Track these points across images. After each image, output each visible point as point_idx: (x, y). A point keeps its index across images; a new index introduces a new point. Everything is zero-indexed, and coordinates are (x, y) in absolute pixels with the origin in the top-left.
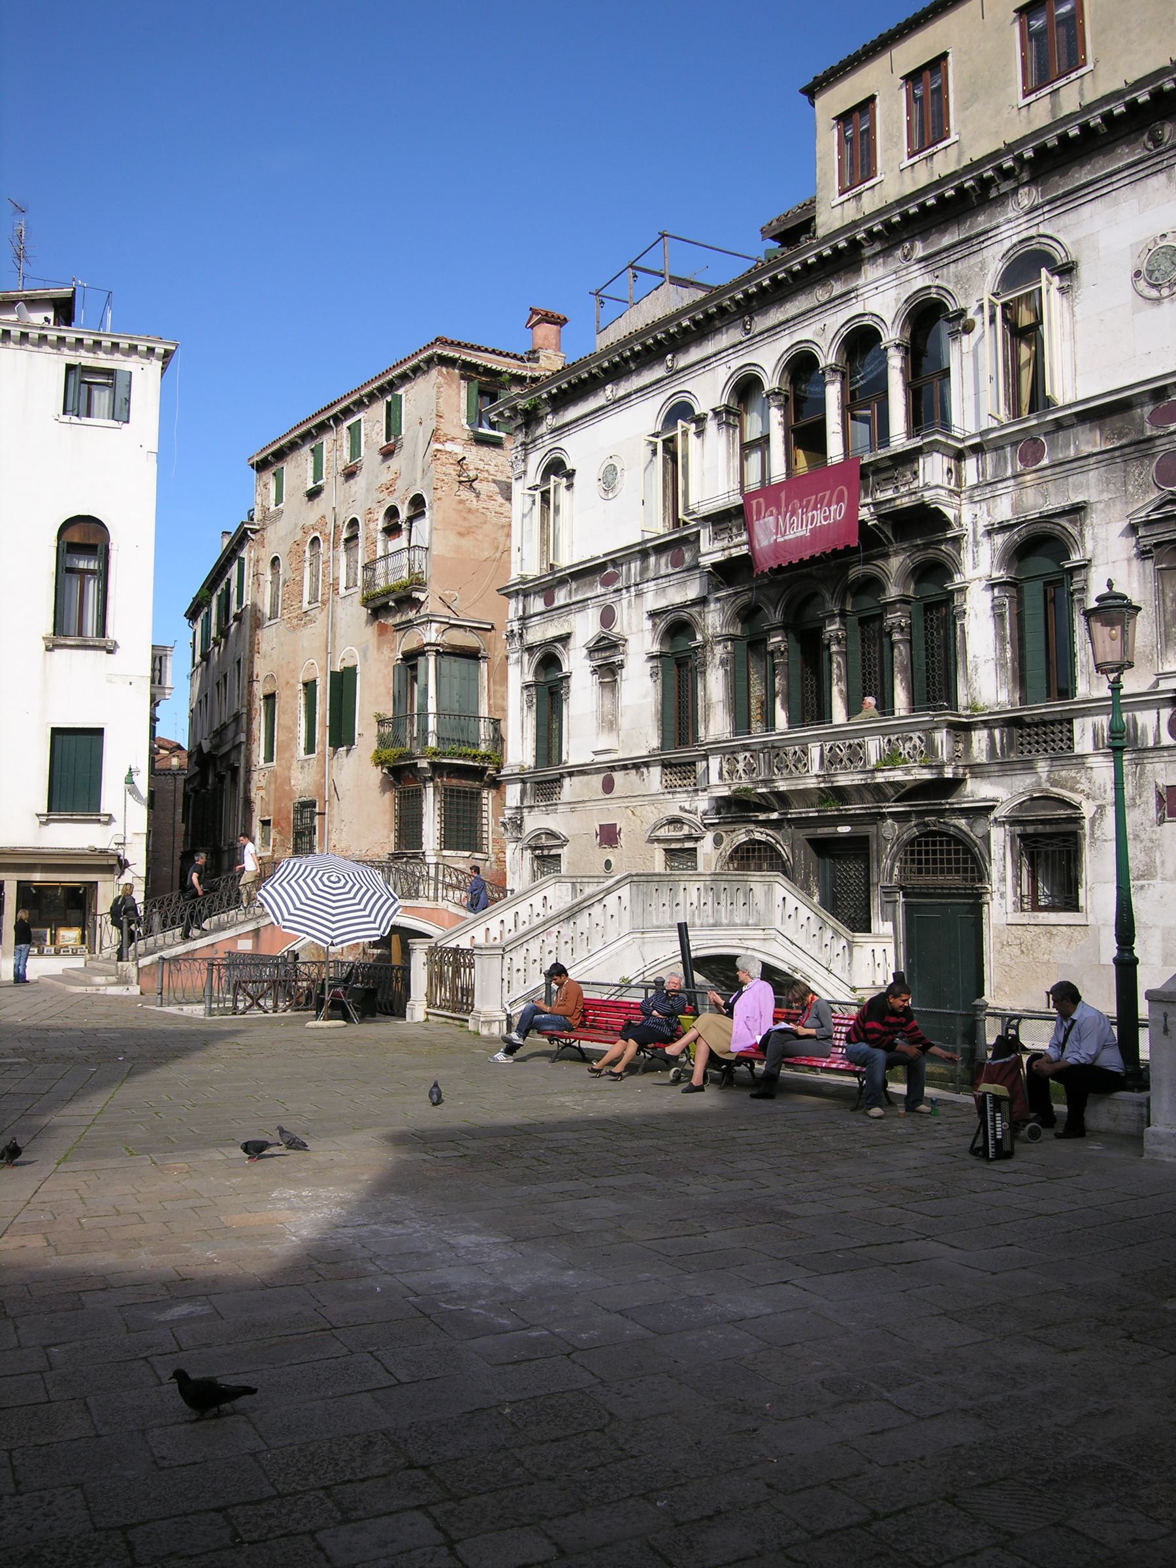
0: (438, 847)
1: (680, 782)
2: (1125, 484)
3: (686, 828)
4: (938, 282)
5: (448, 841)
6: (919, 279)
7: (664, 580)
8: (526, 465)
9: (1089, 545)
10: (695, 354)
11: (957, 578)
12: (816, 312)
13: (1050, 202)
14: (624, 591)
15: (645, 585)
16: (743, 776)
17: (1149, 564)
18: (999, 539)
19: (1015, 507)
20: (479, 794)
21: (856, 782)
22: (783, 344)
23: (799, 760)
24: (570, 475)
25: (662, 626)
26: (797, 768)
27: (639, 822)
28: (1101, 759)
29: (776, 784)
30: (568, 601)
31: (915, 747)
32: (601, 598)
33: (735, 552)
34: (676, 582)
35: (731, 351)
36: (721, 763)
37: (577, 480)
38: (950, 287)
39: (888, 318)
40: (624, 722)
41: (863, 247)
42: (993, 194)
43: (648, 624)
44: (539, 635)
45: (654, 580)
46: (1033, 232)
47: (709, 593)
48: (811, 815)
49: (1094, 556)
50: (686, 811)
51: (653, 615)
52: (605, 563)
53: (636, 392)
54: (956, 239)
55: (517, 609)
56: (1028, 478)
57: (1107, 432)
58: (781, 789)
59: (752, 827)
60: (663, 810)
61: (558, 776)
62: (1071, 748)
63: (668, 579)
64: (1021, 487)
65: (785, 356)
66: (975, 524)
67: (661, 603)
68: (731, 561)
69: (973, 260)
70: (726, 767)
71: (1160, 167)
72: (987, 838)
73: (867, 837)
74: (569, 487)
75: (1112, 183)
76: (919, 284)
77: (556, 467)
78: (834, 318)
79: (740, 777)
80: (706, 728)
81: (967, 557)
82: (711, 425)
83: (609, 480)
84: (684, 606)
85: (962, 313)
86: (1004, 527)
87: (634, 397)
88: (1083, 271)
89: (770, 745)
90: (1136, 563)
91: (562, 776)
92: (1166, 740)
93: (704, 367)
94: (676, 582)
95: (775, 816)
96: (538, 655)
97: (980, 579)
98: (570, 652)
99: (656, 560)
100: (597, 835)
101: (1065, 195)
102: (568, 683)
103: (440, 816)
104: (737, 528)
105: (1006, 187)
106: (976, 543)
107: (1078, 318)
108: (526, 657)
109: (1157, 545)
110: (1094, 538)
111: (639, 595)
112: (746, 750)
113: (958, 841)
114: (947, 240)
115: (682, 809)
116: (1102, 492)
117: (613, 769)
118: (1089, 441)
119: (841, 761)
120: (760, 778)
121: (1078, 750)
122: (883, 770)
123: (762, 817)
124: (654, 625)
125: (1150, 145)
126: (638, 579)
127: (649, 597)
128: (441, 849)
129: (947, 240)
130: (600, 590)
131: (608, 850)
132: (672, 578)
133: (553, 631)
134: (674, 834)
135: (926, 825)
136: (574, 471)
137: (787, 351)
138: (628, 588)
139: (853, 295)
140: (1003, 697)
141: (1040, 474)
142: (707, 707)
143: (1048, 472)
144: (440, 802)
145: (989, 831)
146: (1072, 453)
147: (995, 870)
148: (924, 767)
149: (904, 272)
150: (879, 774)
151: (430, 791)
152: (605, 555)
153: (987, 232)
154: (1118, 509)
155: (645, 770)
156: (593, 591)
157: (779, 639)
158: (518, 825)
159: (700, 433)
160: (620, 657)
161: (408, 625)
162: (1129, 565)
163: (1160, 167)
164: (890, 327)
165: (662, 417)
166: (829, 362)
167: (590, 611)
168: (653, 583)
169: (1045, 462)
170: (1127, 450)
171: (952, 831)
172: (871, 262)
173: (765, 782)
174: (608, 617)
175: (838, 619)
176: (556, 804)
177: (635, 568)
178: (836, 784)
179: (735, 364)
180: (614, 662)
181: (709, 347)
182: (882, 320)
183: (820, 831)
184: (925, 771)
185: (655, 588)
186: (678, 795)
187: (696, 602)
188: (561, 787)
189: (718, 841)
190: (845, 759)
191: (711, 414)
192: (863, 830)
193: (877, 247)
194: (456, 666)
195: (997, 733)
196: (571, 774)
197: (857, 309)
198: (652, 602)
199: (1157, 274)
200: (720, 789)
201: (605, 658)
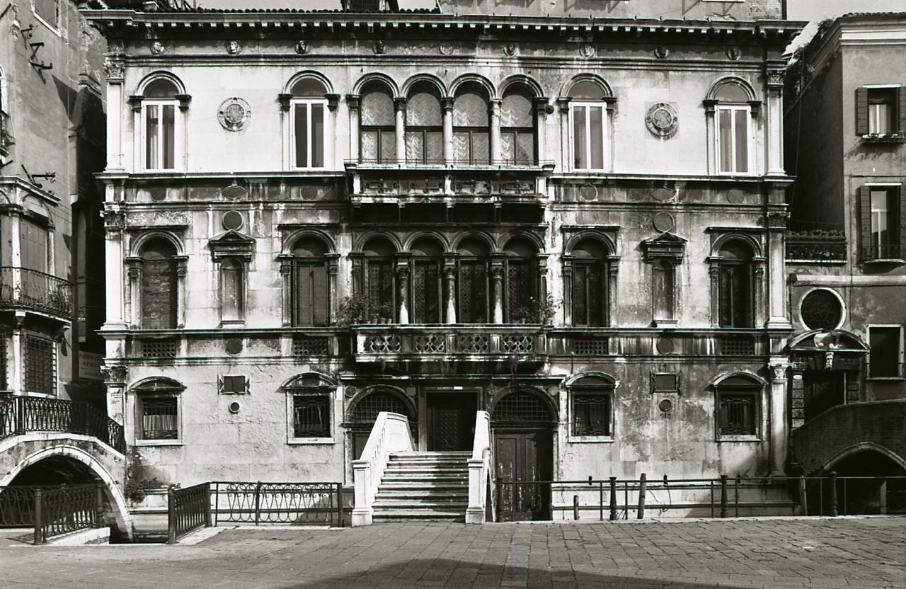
0: (23, 388)
2: (639, 223)
4: (529, 76)
5: (31, 383)
8: (125, 75)
9: (619, 249)
10: (324, 50)
11: (542, 250)
15: (276, 205)
17: (650, 266)
18: (568, 235)
19: (579, 219)
20: (51, 345)
22: (412, 71)
24: (185, 100)
25: (293, 236)
30: (182, 200)
35: (364, 59)
37: (192, 105)
38: (539, 83)
39: (496, 84)
41: (482, 33)
44: (145, 220)
45: (284, 202)
46: (591, 72)
47: (341, 222)
49: (622, 256)
53: (265, 57)
54: (543, 56)
55: (116, 196)
56: (587, 206)
57: (633, 194)
64: (582, 210)
65: (412, 80)
66: (553, 223)
69: (553, 72)
71: (662, 68)
74: (184, 109)
75: (637, 65)
76: (517, 71)
77: (162, 87)
78: (454, 69)
79: (386, 351)
81: (548, 240)
82: (343, 107)
84: (320, 226)
85: (547, 100)
86: (572, 229)
87: (262, 60)
88: (621, 104)
90: (643, 264)
93: (338, 62)
97: (555, 255)
98: (188, 242)
101: (612, 60)
103: (25, 361)
105: (577, 40)
107: (616, 129)
108: (128, 237)
109: (656, 258)
110: (622, 246)
111: (268, 210)
113: (535, 397)
114: (537, 54)
116: (627, 224)
118: (621, 196)
125: (658, 55)
127: (279, 213)
128: (27, 391)
129: (537, 54)
133: (162, 221)
136: (190, 97)
137: (414, 77)
138: (256, 204)
139: (470, 60)
140: (568, 320)
144: (25, 348)
145: (559, 393)
146: (611, 199)
147: (562, 414)
149: (508, 61)
151: (16, 338)
152: (235, 173)
154: (635, 234)
156: (214, 197)
157: (406, 264)
158: (121, 372)
159: (333, 108)
162: (640, 264)
163: (662, 68)
164: (496, 90)
165: (292, 84)
166: (449, 95)
167: (210, 213)
169: (596, 200)
170: (641, 207)
171: (534, 391)
172: (483, 45)
174: (231, 221)
179: (367, 70)
181: (343, 51)
183: (439, 388)
187: (327, 226)
191: (343, 98)
193: (490, 38)
194: (35, 231)
195: (564, 340)
197: (472, 69)
199: (659, 123)
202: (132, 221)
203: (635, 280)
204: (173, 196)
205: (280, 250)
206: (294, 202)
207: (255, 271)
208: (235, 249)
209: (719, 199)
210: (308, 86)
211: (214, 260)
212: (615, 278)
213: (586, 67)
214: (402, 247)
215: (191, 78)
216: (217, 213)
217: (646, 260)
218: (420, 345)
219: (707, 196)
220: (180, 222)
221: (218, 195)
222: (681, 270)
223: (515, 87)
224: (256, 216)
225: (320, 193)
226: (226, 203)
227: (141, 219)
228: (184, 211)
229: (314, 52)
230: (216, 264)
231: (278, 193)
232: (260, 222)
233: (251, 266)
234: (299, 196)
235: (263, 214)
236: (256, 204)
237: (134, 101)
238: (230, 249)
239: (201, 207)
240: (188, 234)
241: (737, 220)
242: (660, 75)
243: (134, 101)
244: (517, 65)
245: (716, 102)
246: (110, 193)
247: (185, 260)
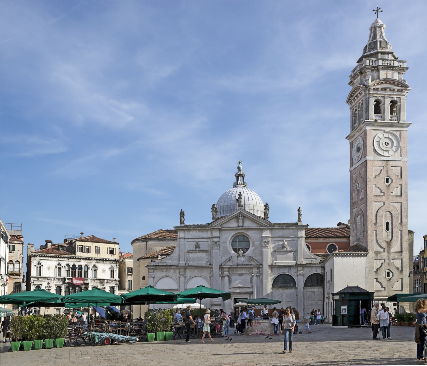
6: (86, 263)
10: (61, 259)
19: (93, 284)
25: (57, 286)
33: (70, 282)
55: (33, 279)
67: (56, 284)
68: (69, 283)
81: (89, 287)
83: (49, 268)
96: (36, 286)
108: (34, 285)
118: (98, 281)
130: (47, 280)
133: (39, 283)
161: (18, 278)
174: (49, 283)
192: (79, 308)
198: (55, 283)
202: (35, 283)
204: (40, 279)
209: (111, 282)
210: (59, 264)
215: (43, 262)
219: (109, 281)
223: (86, 266)
227: (35, 283)
229: (60, 260)
237: (35, 265)
240: (42, 285)
242: (104, 265)
243: (35, 265)
246: (32, 279)
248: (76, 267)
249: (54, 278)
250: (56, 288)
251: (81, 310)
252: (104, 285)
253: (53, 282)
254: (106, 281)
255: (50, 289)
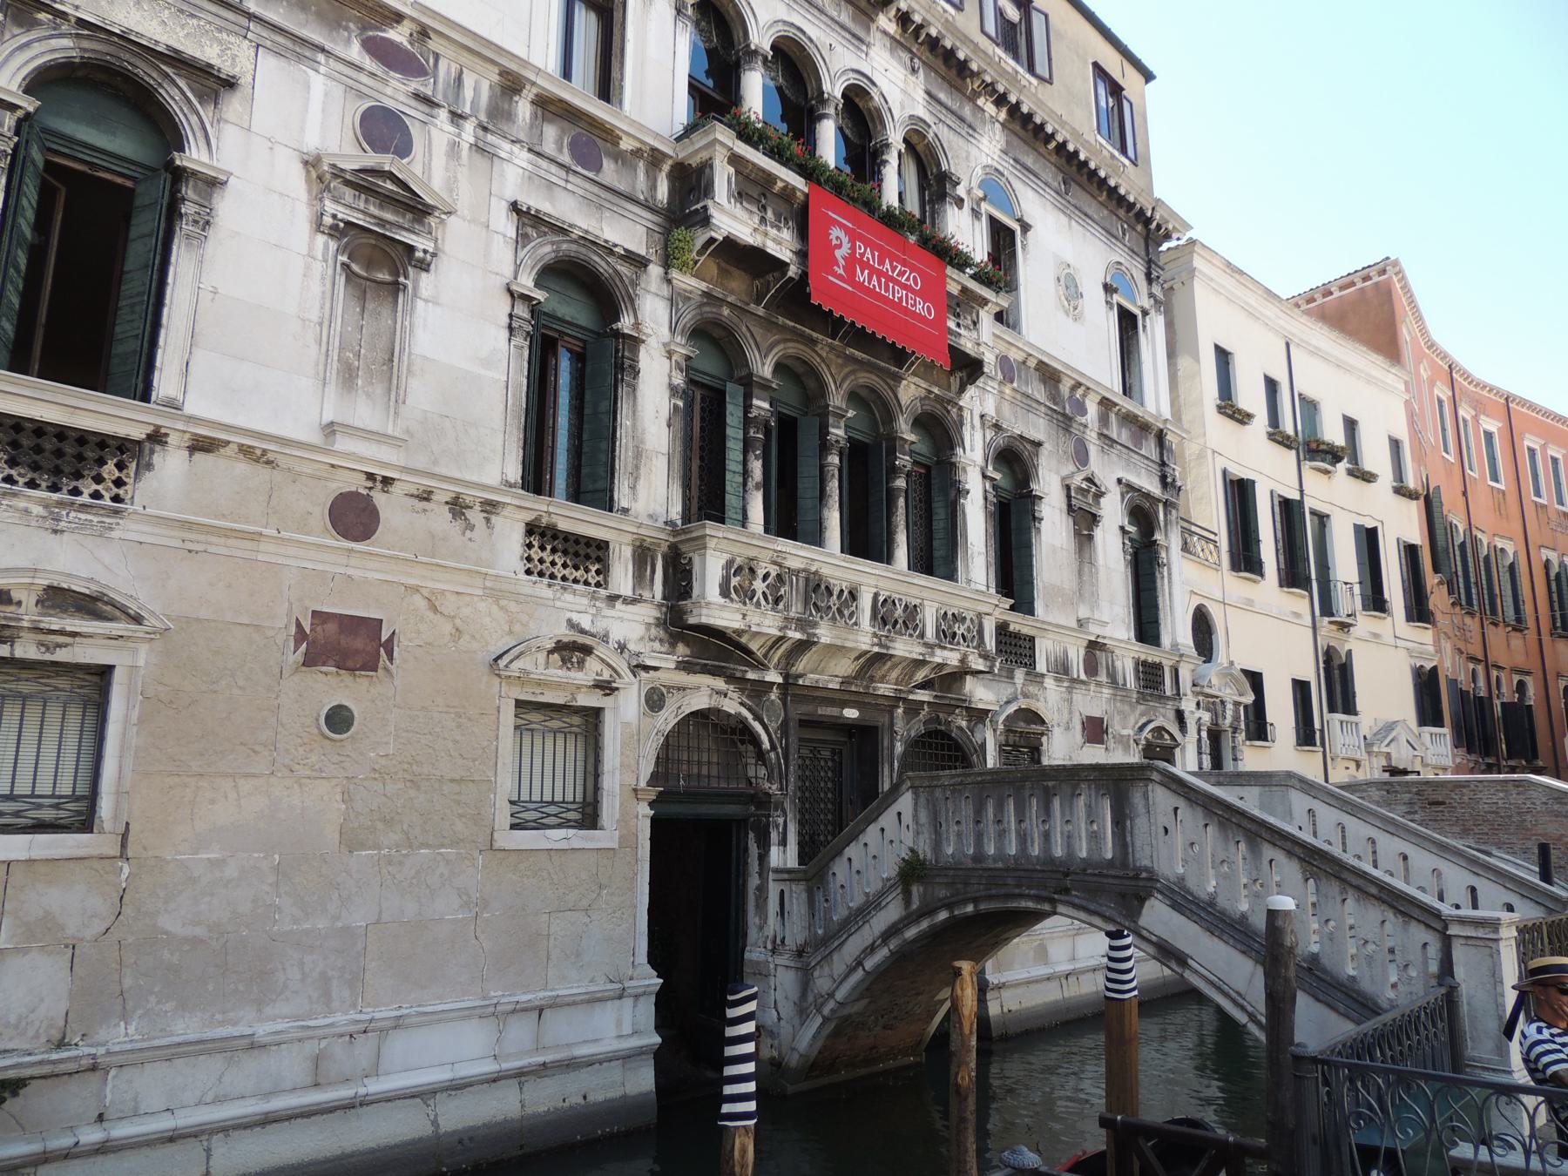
1: (566, 572)
3: (592, 664)
7: (554, 169)
11: (959, 451)
12: (823, 18)
13: (1015, 160)
14: (443, 114)
15: (506, 146)
16: (763, 602)
18: (990, 434)
19: (998, 410)
21: (916, 656)
23: (846, 604)
25: (544, 250)
26: (840, 611)
27: (448, 628)
28: (1052, 681)
29: (817, 631)
31: (969, 630)
32: (364, 79)
33: (772, 249)
34: (581, 192)
36: (729, 564)
40: (420, 393)
42: (981, 102)
43: (506, 226)
45: (530, 150)
48: (830, 686)
50: (583, 631)
51: (528, 220)
52: (398, 17)
58: (823, 640)
59: (720, 683)
60: (524, 618)
61: (138, 433)
62: (1033, 664)
63: (563, 174)
65: (780, 27)
69: (961, 142)
70: (735, 581)
72: (983, 746)
73: (876, 728)
76: (921, 112)
79: (758, 604)
80: (633, 488)
89: (813, 569)
90: (1065, 515)
91: (157, 438)
92: (1083, 677)
94: (581, 192)
95: (774, 677)
99: (535, 116)
100: (301, 635)
102: (209, 197)
104: (774, 214)
105: (990, 108)
106: (973, 427)
112: (775, 563)
114: (942, 96)
115: (572, 625)
117: (387, 481)
118: (1039, 392)
119: (896, 622)
120: (792, 614)
121: (1038, 669)
122: (945, 648)
123: (751, 675)
124: (522, 239)
126: (483, 118)
130: (355, 52)
131: (332, 680)
132: (571, 178)
134: (560, 672)
135: (938, 720)
137: (785, 22)
139: (864, 48)
141: (1014, 394)
142: (638, 455)
143: (1019, 397)
148: (980, 656)
150: (938, 652)
153: (975, 130)
155: (475, 516)
156: (333, 41)
160: (430, 247)
168: (525, 155)
173: (802, 624)
175: (842, 424)
176: (117, 512)
177: (476, 89)
178: (891, 652)
180: (411, 249)
182: (890, 109)
184: (981, 661)
185: (530, 167)
186: (568, 597)
187: (631, 258)
188: (149, 466)
189: (655, 701)
190: (900, 621)
193: (892, 28)
196: (201, 446)
200: (726, 615)
201: (382, 222)
203: (1058, 544)
205: (508, 271)
206: (552, 160)
207: (436, 303)
208: (389, 216)
209: (1124, 436)
211: (318, 226)
212: (1038, 530)
213: (996, 157)
214: (763, 364)
216: (338, 91)
217: (1070, 508)
218: (819, 603)
220: (208, 52)
221: (348, 41)
222: (1098, 533)
224: (454, 147)
225: (610, 172)
226: (372, 75)
228: (230, 32)
230: (321, 239)
231: (509, 116)
232: (463, 174)
233: (426, 283)
234: (560, 150)
235: (470, 157)
236: (457, 117)
238: (373, 210)
239: (301, 49)
240: (233, 105)
241: (1139, 475)
244: (921, 101)
245: (1115, 291)
247: (213, 184)
248: (826, 87)
249: (511, 84)
250: (526, 283)
251: (899, 748)
252: (1082, 457)
253: (479, 148)
254: (1092, 408)
255: (420, 243)
